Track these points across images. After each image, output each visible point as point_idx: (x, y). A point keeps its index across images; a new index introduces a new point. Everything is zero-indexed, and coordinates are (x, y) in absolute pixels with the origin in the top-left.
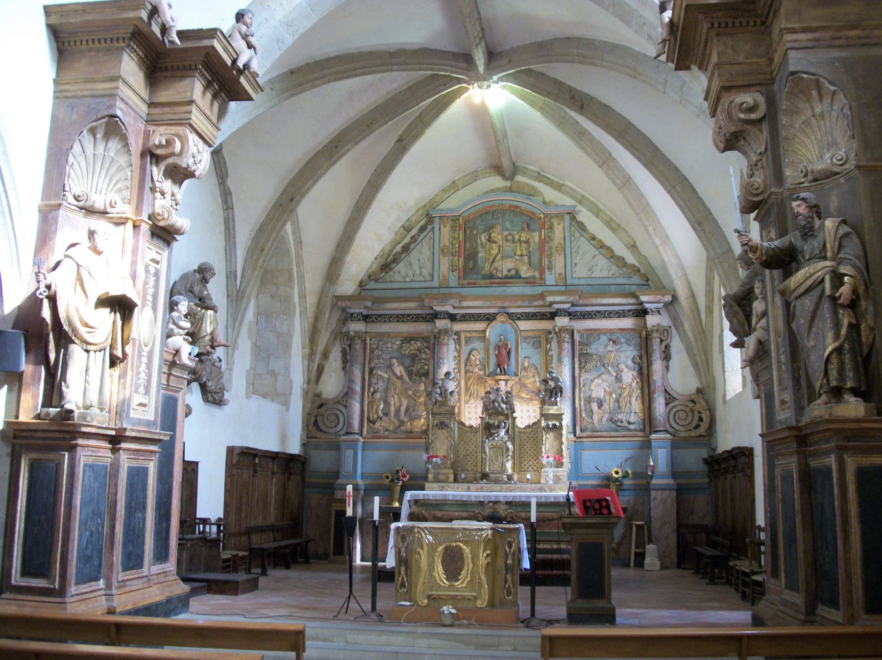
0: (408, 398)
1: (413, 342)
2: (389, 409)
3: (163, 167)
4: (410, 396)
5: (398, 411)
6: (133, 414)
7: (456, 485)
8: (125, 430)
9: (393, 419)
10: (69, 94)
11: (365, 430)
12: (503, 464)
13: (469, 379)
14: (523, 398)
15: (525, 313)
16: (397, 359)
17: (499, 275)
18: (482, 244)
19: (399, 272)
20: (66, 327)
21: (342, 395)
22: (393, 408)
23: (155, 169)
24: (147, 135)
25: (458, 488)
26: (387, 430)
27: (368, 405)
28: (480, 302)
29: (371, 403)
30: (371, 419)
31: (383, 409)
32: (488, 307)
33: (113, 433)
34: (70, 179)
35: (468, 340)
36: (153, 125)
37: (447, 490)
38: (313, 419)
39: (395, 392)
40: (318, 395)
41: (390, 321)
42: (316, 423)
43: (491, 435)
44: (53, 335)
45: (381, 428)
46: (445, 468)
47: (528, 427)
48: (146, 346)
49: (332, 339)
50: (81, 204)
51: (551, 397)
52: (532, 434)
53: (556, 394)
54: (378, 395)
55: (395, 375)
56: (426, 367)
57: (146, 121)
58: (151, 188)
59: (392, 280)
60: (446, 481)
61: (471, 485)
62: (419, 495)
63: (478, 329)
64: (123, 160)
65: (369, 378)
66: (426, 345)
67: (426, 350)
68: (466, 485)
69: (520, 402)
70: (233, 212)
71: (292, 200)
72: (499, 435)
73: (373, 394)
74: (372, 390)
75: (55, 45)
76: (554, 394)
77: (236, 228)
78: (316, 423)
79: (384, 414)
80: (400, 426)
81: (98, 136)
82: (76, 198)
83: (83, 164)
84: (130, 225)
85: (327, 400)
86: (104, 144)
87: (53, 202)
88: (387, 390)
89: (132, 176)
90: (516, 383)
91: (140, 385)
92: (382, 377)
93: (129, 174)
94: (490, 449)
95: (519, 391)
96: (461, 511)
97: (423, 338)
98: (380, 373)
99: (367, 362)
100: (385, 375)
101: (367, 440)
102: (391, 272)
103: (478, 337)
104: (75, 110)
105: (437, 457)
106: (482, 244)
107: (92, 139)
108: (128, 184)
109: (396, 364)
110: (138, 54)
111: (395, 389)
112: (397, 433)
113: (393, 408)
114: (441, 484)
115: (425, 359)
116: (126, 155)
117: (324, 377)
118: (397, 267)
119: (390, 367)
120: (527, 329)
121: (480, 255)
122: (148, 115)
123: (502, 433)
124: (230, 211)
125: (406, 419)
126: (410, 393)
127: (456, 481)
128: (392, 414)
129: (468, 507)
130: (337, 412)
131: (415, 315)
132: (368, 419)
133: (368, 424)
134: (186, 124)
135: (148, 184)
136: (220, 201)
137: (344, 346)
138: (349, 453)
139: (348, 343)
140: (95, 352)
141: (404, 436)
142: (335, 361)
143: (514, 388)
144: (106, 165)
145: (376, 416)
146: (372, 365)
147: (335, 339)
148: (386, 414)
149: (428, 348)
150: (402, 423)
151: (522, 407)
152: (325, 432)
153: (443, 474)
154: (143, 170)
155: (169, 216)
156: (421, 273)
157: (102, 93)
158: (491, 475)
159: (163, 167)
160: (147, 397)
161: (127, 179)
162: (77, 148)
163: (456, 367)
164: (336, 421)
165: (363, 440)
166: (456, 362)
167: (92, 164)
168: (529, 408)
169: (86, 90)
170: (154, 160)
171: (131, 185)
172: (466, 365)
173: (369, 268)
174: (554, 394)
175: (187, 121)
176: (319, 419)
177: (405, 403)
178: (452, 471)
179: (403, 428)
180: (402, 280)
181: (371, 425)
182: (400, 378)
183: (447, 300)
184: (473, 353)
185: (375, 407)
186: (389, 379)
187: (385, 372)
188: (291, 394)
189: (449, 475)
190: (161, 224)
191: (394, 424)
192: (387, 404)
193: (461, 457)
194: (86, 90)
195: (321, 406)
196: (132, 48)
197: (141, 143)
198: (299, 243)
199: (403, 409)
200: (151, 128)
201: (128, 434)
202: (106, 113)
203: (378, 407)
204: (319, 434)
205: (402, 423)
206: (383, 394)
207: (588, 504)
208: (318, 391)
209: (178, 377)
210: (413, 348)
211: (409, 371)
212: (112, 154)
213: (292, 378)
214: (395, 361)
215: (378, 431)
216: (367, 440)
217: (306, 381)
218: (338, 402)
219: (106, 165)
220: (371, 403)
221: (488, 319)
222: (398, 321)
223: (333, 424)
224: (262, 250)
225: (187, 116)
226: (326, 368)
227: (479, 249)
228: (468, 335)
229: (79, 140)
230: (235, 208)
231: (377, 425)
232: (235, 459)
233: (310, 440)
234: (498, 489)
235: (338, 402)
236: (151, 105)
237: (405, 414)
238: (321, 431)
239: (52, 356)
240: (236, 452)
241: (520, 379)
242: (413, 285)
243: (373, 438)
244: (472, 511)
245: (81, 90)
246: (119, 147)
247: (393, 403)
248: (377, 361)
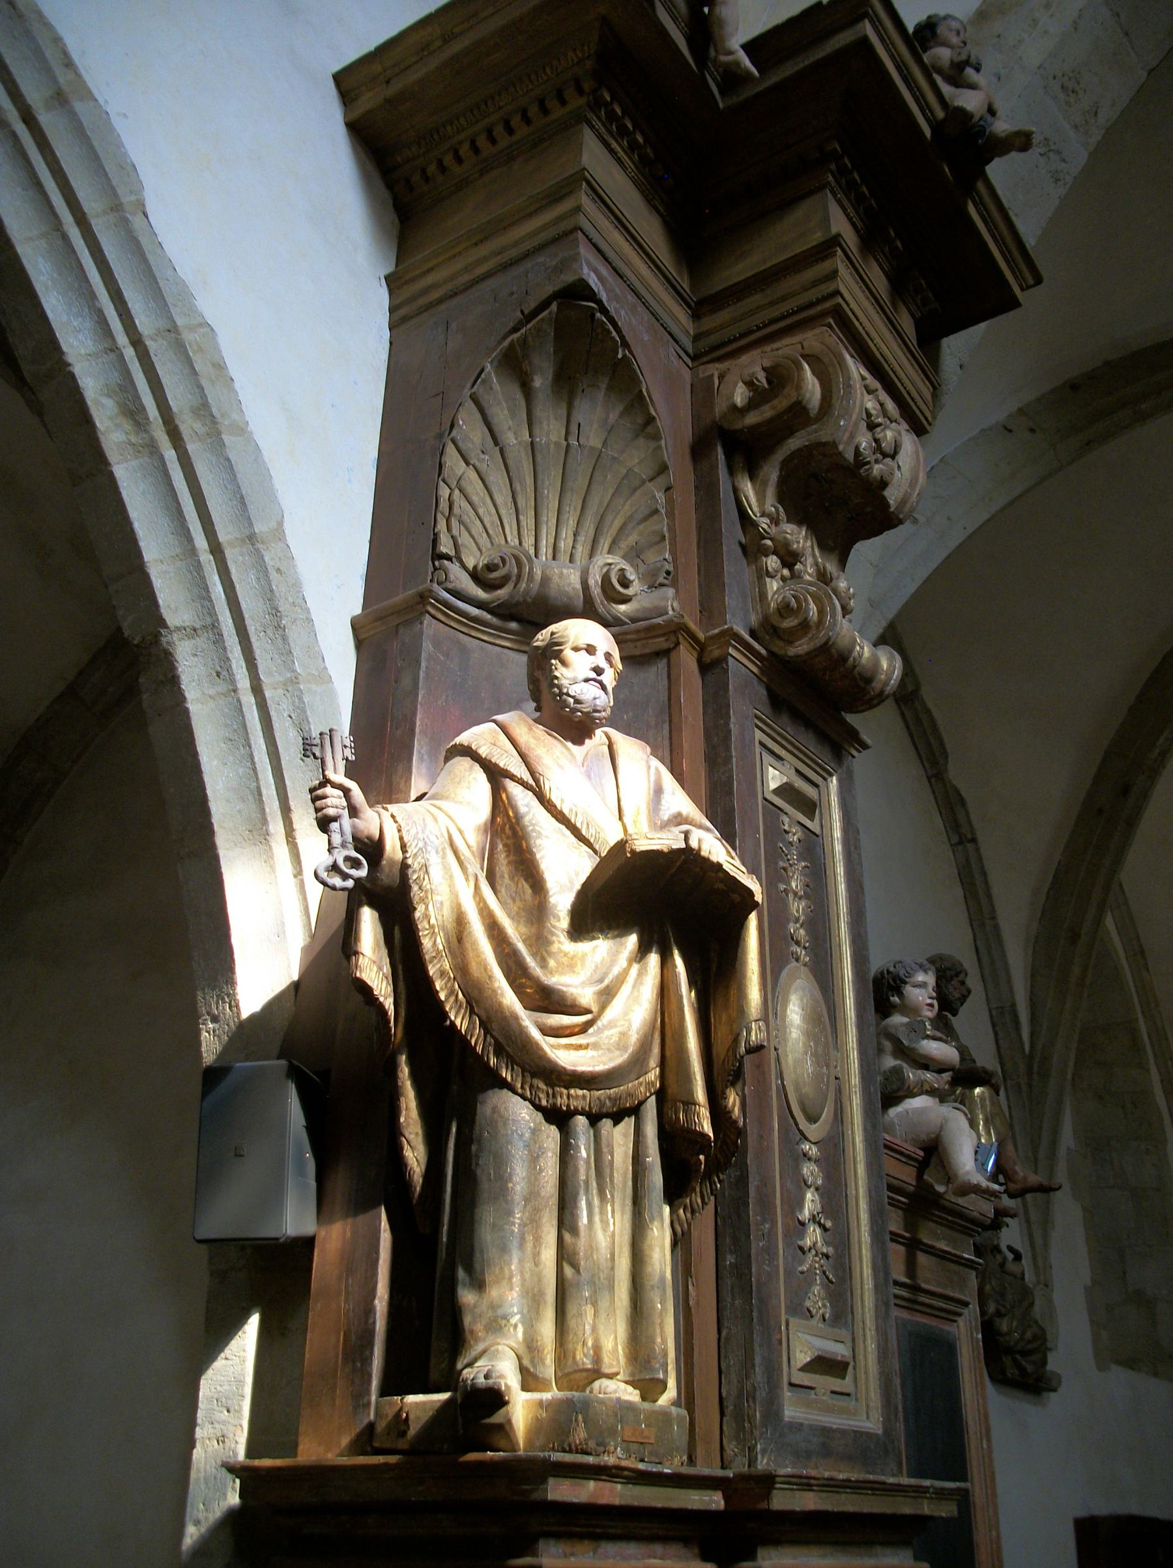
3: (772, 472)
6: (792, 1410)
8: (768, 1481)
10: (435, 295)
20: (459, 1020)
23: (748, 489)
24: (703, 393)
33: (715, 1501)
34: (454, 523)
36: (719, 359)
44: (411, 1062)
48: (812, 1119)
50: (502, 593)
57: (693, 359)
58: (743, 548)
64: (636, 458)
70: (978, 850)
71: (1126, 791)
75: (385, 194)
77: (995, 891)
81: (538, 382)
82: (475, 576)
83: (498, 479)
84: (687, 658)
86: (563, 412)
87: (401, 597)
89: (670, 502)
91: (807, 1279)
93: (660, 496)
104: (454, 326)
107: (519, 396)
108: (662, 525)
110: (633, 147)
116: (641, 441)
122: (696, 338)
124: (970, 846)
134: (823, 315)
135: (732, 533)
136: (938, 821)
140: (594, 1119)
144: (579, 481)
154: (707, 491)
155: (821, 612)
157: (527, 246)
159: (772, 472)
160: (844, 1333)
161: (656, 511)
162: (470, 429)
167: (529, 481)
169: (485, 259)
170: (739, 461)
171: (671, 529)
175: (828, 305)
190: (801, 647)
194: (485, 259)
196: (611, 116)
197: (686, 415)
198: (1139, 954)
200: (714, 370)
201: (781, 1501)
202: (550, 289)
209: (941, 1255)
212: (594, 440)
219: (579, 481)
224: (1074, 937)
225: (829, 287)
229: (475, 399)
230: (980, 837)
236: (699, 309)
239: (415, 1156)
245: (467, 269)
246: (613, 416)
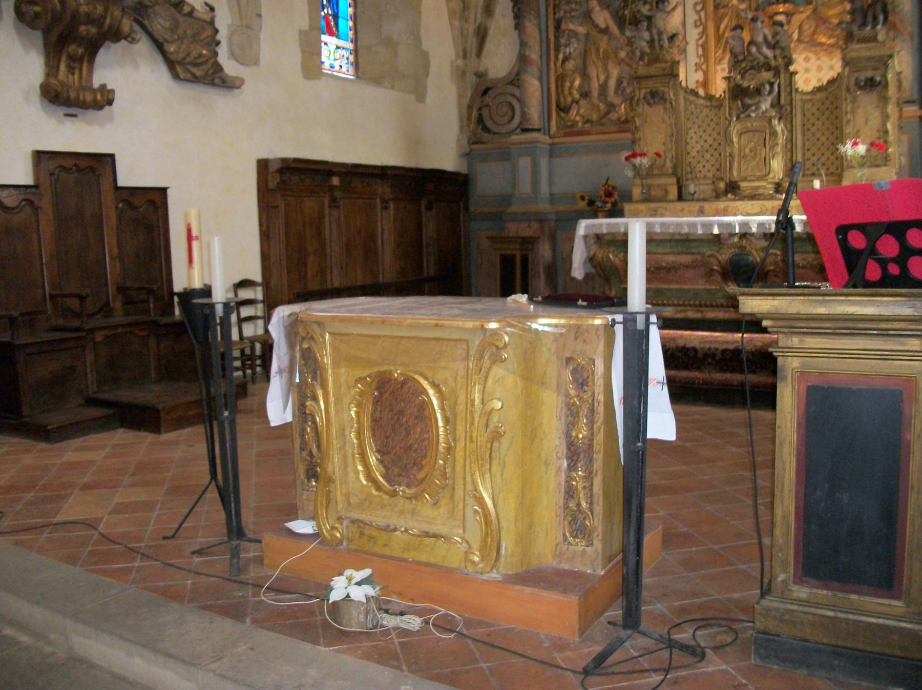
0: (619, 64)
2: (589, 86)
4: (622, 60)
5: (604, 87)
7: (679, 205)
9: (596, 101)
11: (554, 123)
12: (766, 162)
13: (721, 20)
14: (821, 44)
22: (595, 86)
25: (682, 210)
26: (587, 121)
27: (557, 82)
29: (560, 79)
30: (563, 105)
31: (580, 87)
37: (662, 215)
38: (475, 113)
39: (598, 56)
40: (480, 75)
42: (480, 120)
43: (746, 107)
45: (578, 118)
46: (661, 175)
47: (819, 89)
51: (864, 24)
52: (827, 104)
53: (875, 18)
54: (570, 65)
55: (597, 26)
60: (663, 199)
61: (706, 205)
62: (601, 225)
65: (557, 38)
68: (696, 206)
69: (816, 53)
72: (757, 108)
73: (563, 62)
74: (561, 56)
76: (870, 19)
78: (480, 120)
79: (581, 95)
80: (608, 113)
85: (497, 81)
88: (585, 55)
90: (808, 17)
92: (576, 34)
94: (740, 135)
95: (814, 33)
96: (678, 253)
98: (571, 26)
99: (551, 10)
100: (581, 30)
101: (556, 140)
105: (643, 155)
109: (598, 8)
111: (598, 50)
112: (603, 125)
113: (595, 86)
114: (652, 205)
117: (489, 45)
119: (588, 16)
123: (765, 105)
125: (616, 100)
126: (623, 54)
127: (680, 198)
128: (595, 93)
129: (692, 244)
130: (510, 99)
132: (557, 106)
133: (558, 114)
138: (524, 163)
141: (617, 130)
142: (503, 16)
143: (806, 27)
145: (569, 99)
146: (557, 15)
148: (585, 95)
150: (611, 107)
151: (819, 62)
152: (495, 133)
153: (659, 186)
158: (743, 185)
164: (510, 113)
165: (550, 141)
168: (833, 62)
174: (870, 19)
176: (485, 112)
177: (614, 72)
178: (674, 180)
179: (613, 116)
181: (563, 115)
182: (605, 31)
185: (568, 84)
186: (587, 36)
187: (582, 24)
188: (427, 74)
189: (669, 188)
191: (599, 110)
192: (585, 76)
193: (693, 153)
195: (486, 92)
199: (612, 83)
203: (572, 83)
204: (486, 136)
205: (611, 107)
207: (857, 241)
208: (482, 69)
211: (621, 18)
213: (426, 46)
215: (575, 123)
216: (556, 140)
217: (461, 54)
220: (560, 79)
223: (506, 119)
226: (491, 32)
231: (573, 112)
232: (273, 182)
233: (475, 147)
234: (757, 210)
237: (616, 92)
240: (273, 168)
241: (815, 11)
243: (567, 135)
244: (699, 253)
247: (595, 74)
248: (567, 8)
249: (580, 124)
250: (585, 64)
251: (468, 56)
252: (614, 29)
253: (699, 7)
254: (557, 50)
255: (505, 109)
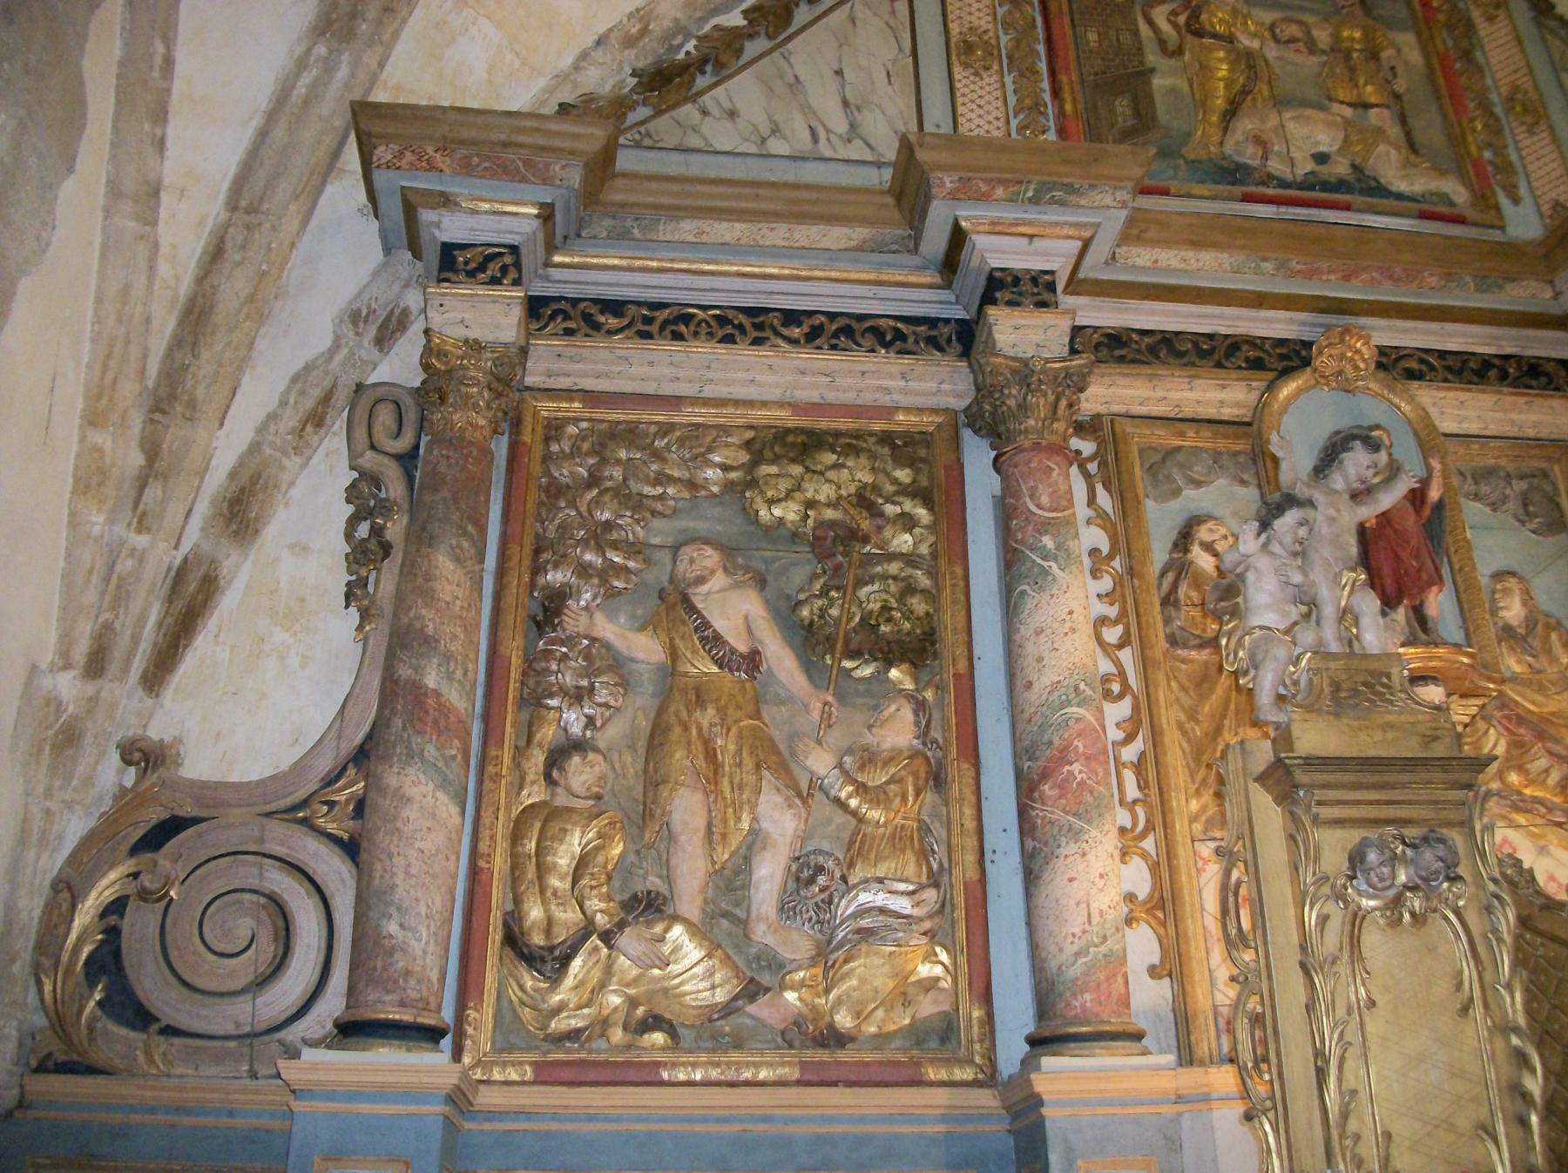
1: (831, 458)
15: (1442, 354)
16: (728, 551)
17: (1276, 166)
18: (1162, 43)
19: (732, 114)
21: (325, 764)
28: (1225, 258)
32: (1259, 301)
35: (1161, 463)
41: (677, 336)
49: (290, 420)
55: (712, 641)
56: (919, 606)
59: (694, 141)
63: (1210, 412)
66: (904, 475)
67: (908, 505)
85: (215, 796)
92: (617, 665)
97: (886, 438)
98: (607, 628)
102: (688, 111)
103: (1217, 455)
106: (1162, 43)
109: (719, 580)
115: (909, 559)
118: (719, 92)
120: (1473, 427)
121: (1158, 82)
125: (796, 944)
131: (832, 316)
137: (369, 459)
139: (403, 444)
141: (795, 1074)
145: (569, 916)
147: (317, 419)
149: (924, 496)
152: (171, 1031)
156: (853, 126)
163: (1113, 612)
164: (266, 949)
166: (1106, 584)
172: (1169, 601)
173: (561, 78)
176: (140, 925)
180: (753, 149)
183: (1070, 189)
184: (1203, 533)
186: (670, 672)
195: (170, 827)
199: (769, 874)
206: (632, 764)
210: (825, 492)
214: (710, 557)
218: (298, 814)
221: (1256, 365)
222: (728, 339)
223: (242, 970)
226: (228, 602)
227: (1152, 57)
228: (1164, 437)
235: (298, 814)
237: (787, 908)
238: (141, 1017)
242: (812, 173)
249: (617, 1035)
250: (654, 781)
251: (113, 669)
252: (781, 660)
253: (1112, 635)
254: (534, 701)
255: (244, 927)
